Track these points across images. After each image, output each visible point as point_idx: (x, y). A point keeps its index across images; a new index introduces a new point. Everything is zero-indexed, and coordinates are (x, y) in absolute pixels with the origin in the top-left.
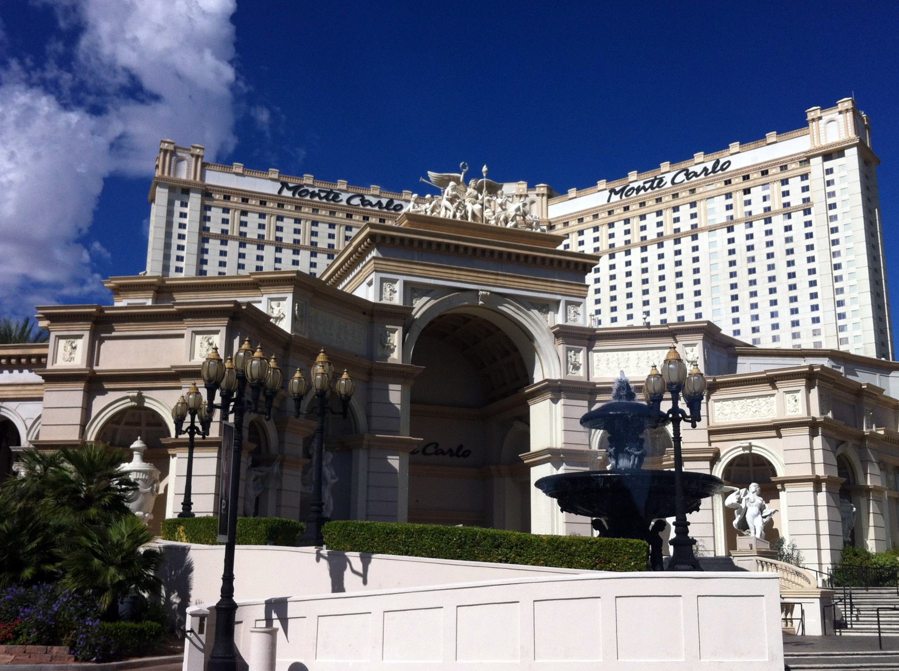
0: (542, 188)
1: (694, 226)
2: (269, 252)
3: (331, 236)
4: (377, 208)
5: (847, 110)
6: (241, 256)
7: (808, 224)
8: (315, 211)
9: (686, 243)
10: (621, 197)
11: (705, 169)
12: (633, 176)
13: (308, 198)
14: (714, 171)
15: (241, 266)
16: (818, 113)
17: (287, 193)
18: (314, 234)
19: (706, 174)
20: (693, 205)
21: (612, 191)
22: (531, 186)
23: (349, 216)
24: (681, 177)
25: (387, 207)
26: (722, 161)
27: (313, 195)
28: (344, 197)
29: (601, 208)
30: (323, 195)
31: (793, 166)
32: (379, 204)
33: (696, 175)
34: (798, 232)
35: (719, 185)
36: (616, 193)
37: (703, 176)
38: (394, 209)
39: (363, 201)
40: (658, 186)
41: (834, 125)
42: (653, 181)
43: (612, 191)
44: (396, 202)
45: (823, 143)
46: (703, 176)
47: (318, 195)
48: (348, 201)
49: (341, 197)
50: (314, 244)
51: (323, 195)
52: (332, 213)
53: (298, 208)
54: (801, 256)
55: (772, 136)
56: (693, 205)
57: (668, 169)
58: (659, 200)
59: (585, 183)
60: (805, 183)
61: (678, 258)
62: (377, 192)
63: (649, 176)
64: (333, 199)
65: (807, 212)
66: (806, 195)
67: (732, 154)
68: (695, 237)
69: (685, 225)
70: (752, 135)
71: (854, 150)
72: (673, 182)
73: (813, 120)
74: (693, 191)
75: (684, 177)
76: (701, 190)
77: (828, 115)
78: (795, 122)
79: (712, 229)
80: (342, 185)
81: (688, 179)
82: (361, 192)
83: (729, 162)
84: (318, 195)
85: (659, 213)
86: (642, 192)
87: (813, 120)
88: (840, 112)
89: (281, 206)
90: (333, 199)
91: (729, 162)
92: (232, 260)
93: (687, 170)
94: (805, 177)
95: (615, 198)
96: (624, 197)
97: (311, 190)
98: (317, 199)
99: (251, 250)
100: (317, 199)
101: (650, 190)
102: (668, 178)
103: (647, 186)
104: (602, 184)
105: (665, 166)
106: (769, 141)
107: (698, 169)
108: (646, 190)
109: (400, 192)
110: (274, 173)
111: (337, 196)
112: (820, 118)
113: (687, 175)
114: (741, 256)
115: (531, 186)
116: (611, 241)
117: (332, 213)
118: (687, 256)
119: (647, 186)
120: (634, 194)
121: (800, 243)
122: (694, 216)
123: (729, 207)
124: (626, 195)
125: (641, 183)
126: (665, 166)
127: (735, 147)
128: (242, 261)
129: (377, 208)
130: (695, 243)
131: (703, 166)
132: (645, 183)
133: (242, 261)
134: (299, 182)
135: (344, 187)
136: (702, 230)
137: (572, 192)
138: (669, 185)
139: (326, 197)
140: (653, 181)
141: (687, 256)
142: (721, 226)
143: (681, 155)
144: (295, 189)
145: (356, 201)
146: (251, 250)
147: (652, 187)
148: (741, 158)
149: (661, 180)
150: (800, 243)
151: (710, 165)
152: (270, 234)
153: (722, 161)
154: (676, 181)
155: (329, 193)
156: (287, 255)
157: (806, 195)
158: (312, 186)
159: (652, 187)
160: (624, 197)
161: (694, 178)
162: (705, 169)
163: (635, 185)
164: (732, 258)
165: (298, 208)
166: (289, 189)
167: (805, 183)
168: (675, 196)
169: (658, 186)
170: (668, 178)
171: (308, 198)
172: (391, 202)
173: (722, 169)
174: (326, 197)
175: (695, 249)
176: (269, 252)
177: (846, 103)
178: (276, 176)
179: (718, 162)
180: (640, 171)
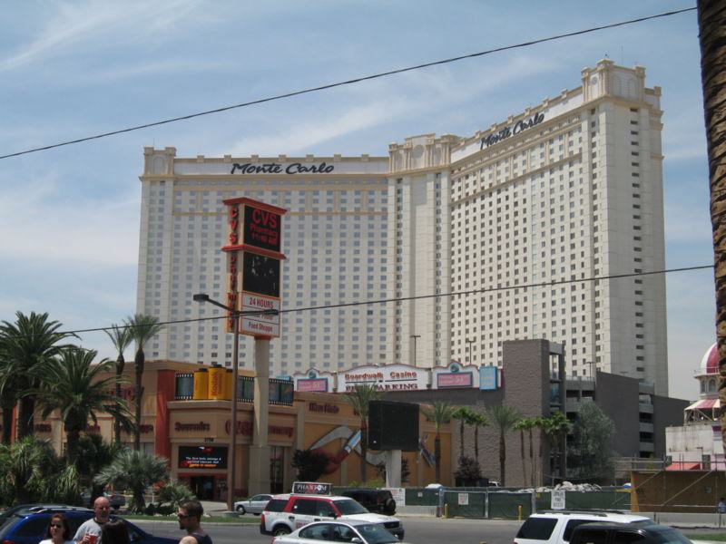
10: (243, 172)
11: (314, 168)
19: (314, 172)
24: (293, 169)
37: (311, 173)
46: (311, 173)
75: (297, 170)
86: (261, 173)
96: (246, 173)
101: (267, 173)
103: (266, 168)
107: (309, 167)
108: (264, 171)
120: (254, 173)
124: (248, 172)
132: (265, 165)
138: (284, 172)
140: (271, 166)
149: (278, 167)
159: (270, 171)
160: (246, 173)
161: (304, 173)
162: (314, 168)
163: (257, 165)
169: (275, 171)
170: (284, 167)
173: (326, 171)
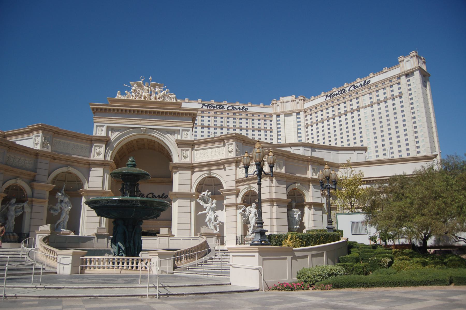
0: (301, 97)
1: (358, 107)
2: (212, 130)
3: (234, 122)
4: (238, 110)
5: (414, 56)
6: (202, 132)
7: (401, 102)
8: (215, 113)
9: (356, 113)
11: (361, 84)
12: (334, 89)
13: (212, 108)
14: (364, 85)
15: (202, 136)
16: (403, 58)
17: (204, 107)
18: (228, 122)
20: (357, 98)
21: (327, 96)
22: (297, 97)
23: (228, 114)
24: (352, 88)
25: (242, 109)
26: (367, 81)
27: (214, 107)
28: (226, 107)
29: (323, 103)
30: (218, 107)
31: (394, 80)
32: (239, 108)
33: (357, 87)
34: (398, 105)
35: (366, 90)
36: (328, 97)
38: (245, 110)
39: (233, 108)
40: (344, 92)
41: (409, 63)
42: (342, 91)
43: (327, 96)
44: (245, 107)
45: (405, 70)
47: (216, 107)
48: (227, 108)
49: (225, 107)
50: (228, 126)
51: (218, 107)
52: (222, 113)
53: (209, 113)
54: (399, 115)
55: (385, 70)
56: (357, 98)
57: (347, 85)
58: (344, 98)
59: (317, 94)
60: (399, 86)
61: (353, 119)
62: (238, 104)
63: (340, 89)
64: (222, 108)
65: (401, 97)
66: (400, 91)
67: (371, 78)
68: (359, 111)
69: (355, 107)
70: (378, 70)
71: (418, 72)
72: (349, 90)
73: (401, 61)
74: (357, 93)
76: (360, 92)
77: (406, 59)
78: (394, 63)
79: (365, 107)
80: (225, 103)
81: (355, 89)
82: (232, 105)
83: (370, 81)
84: (216, 107)
85: (345, 103)
86: (338, 95)
87: (401, 61)
88: (411, 57)
89: (203, 112)
90: (222, 108)
91: (370, 81)
92: (199, 134)
93: (354, 85)
94: (399, 84)
95: (328, 98)
97: (213, 105)
98: (216, 108)
99: (206, 130)
100: (216, 108)
102: (347, 89)
103: (340, 93)
104: (323, 94)
105: (346, 85)
106: (384, 71)
107: (358, 85)
109: (247, 103)
110: (200, 101)
111: (223, 107)
112: (403, 60)
113: (354, 87)
114: (377, 117)
115: (297, 97)
116: (328, 115)
117: (222, 113)
118: (356, 118)
119: (340, 93)
121: (399, 110)
122: (358, 103)
123: (371, 98)
125: (337, 92)
126: (346, 85)
127: (371, 75)
128: (202, 134)
129: (238, 110)
130: (359, 113)
131: (360, 83)
133: (202, 134)
134: (209, 103)
135: (226, 103)
136: (361, 108)
137: (312, 98)
138: (348, 91)
139: (219, 108)
140: (342, 91)
141: (356, 118)
142: (368, 106)
143: (351, 80)
144: (208, 106)
145: (230, 108)
146: (206, 130)
147: (341, 93)
148: (375, 79)
149: (345, 90)
150: (399, 110)
151: (362, 83)
152: (212, 124)
153: (367, 81)
154: (350, 90)
155: (220, 106)
156: (219, 131)
157: (400, 91)
158: (214, 104)
159: (341, 93)
162: (361, 84)
163: (335, 93)
164: (373, 118)
165: (209, 113)
166: (205, 106)
167: (399, 86)
168: (350, 96)
170: (347, 89)
171: (212, 108)
172: (244, 107)
173: (367, 84)
174: (219, 108)
175: (359, 115)
176: (212, 130)
177: (413, 53)
178: (200, 102)
179: (365, 81)
180: (337, 87)
